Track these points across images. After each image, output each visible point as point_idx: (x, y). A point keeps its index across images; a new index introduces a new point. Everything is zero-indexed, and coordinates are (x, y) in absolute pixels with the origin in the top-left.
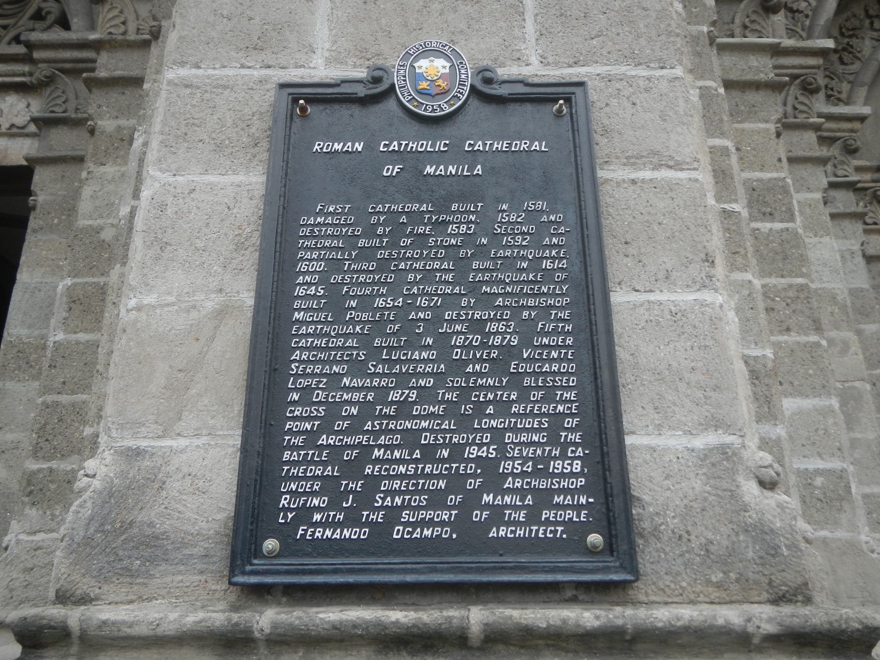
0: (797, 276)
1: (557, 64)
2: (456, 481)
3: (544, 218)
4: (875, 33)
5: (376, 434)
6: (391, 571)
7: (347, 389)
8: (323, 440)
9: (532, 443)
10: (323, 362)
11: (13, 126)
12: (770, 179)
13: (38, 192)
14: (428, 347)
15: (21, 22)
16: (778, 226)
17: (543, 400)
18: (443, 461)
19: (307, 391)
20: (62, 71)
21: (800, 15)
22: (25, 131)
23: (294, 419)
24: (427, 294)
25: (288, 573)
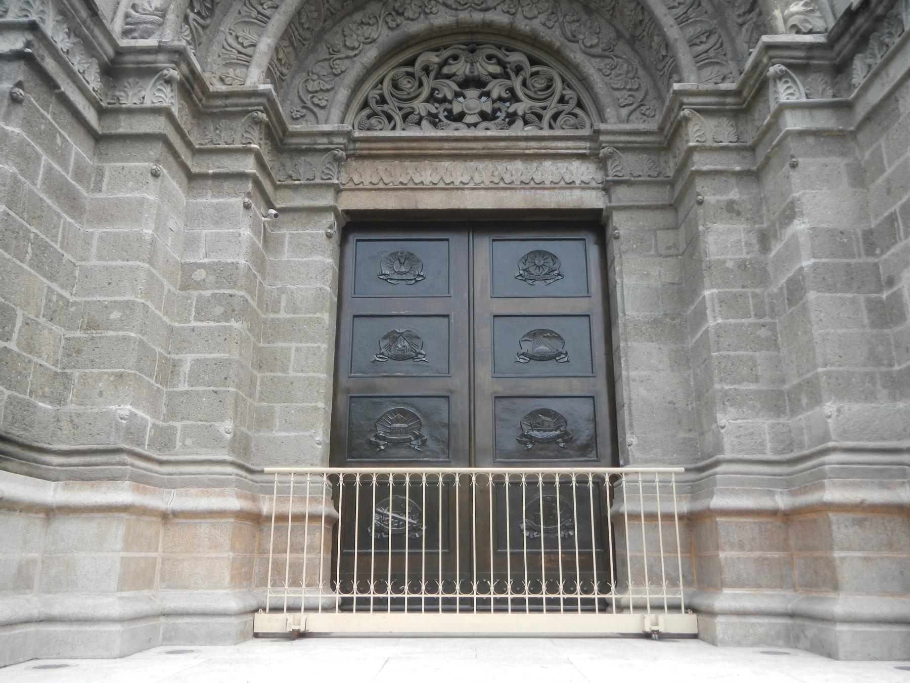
15: (552, 106)
20: (617, 148)
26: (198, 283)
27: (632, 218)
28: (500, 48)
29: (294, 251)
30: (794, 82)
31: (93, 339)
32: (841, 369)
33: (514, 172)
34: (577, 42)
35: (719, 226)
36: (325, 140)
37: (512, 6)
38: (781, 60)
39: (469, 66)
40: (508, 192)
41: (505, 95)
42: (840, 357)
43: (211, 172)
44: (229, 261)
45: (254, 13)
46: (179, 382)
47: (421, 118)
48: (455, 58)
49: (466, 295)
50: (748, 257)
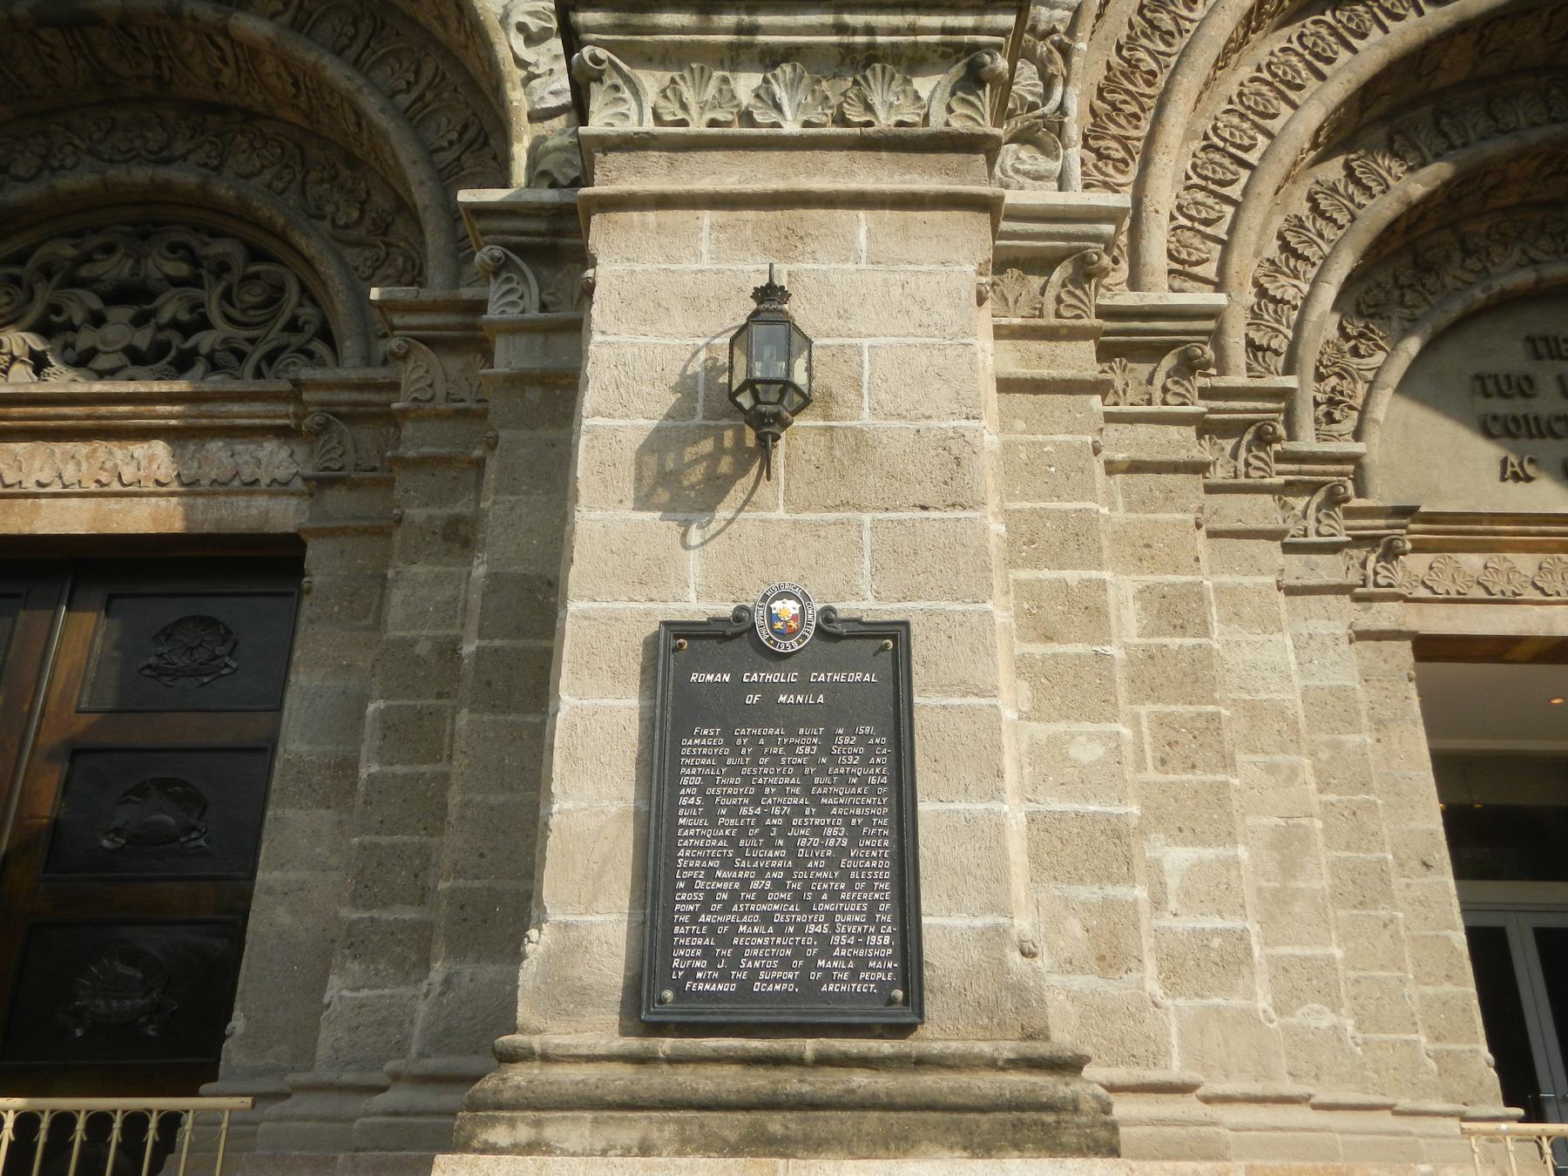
0: (1208, 703)
1: (888, 600)
2: (799, 951)
3: (871, 741)
4: (1406, 311)
5: (741, 915)
6: (752, 1014)
7: (720, 880)
8: (702, 919)
9: (855, 923)
10: (700, 858)
11: (274, 481)
12: (1184, 584)
13: (313, 572)
14: (779, 847)
15: (271, 336)
16: (1190, 641)
17: (865, 890)
18: (790, 935)
19: (691, 881)
20: (337, 415)
21: (1286, 307)
22: (291, 488)
23: (681, 902)
24: (779, 804)
25: (680, 1014)
27: (342, 552)
28: (196, 230)
32: (477, 884)
33: (144, 463)
34: (323, 217)
35: (421, 570)
37: (213, 154)
38: (500, 237)
39: (129, 264)
40: (125, 500)
41: (184, 317)
42: (482, 856)
47: (14, 359)
48: (109, 249)
49: (26, 707)
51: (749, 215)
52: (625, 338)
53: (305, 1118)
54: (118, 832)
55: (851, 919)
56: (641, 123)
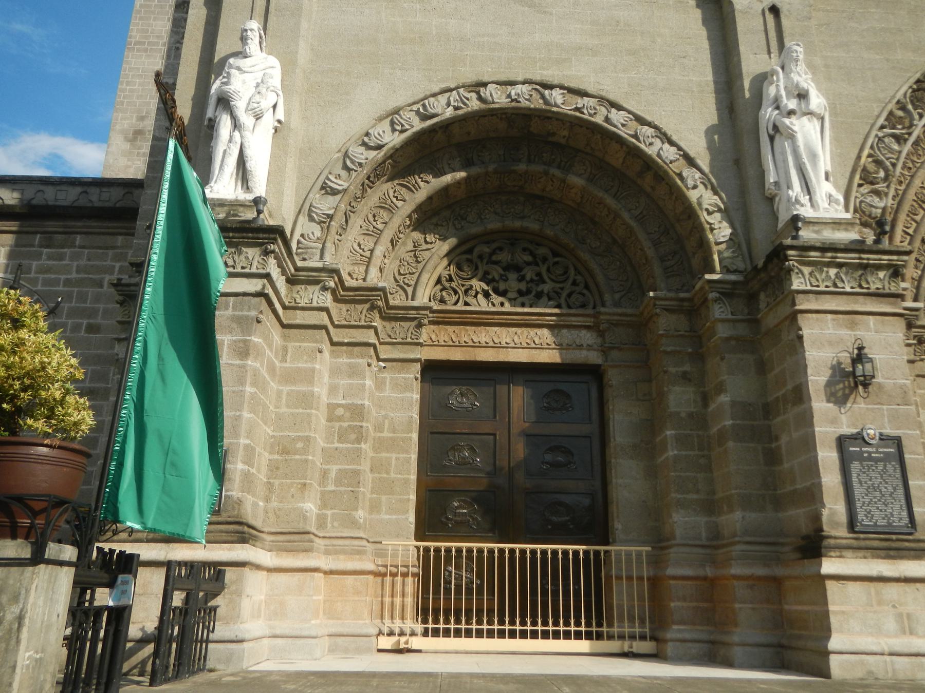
11: (588, 345)
26: (339, 417)
29: (393, 389)
30: (724, 304)
31: (286, 460)
35: (677, 389)
36: (414, 312)
41: (535, 278)
43: (346, 341)
44: (359, 403)
45: (371, 228)
46: (328, 483)
47: (477, 293)
48: (501, 249)
49: (507, 420)
50: (695, 410)
51: (841, 316)
52: (815, 353)
53: (683, 553)
54: (547, 463)
55: (897, 507)
56: (806, 286)
